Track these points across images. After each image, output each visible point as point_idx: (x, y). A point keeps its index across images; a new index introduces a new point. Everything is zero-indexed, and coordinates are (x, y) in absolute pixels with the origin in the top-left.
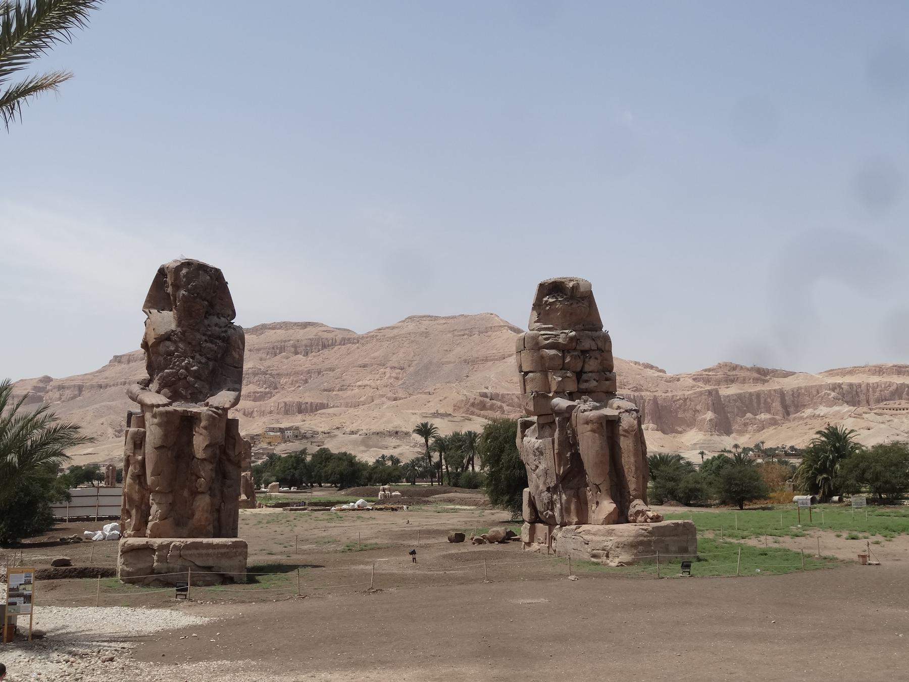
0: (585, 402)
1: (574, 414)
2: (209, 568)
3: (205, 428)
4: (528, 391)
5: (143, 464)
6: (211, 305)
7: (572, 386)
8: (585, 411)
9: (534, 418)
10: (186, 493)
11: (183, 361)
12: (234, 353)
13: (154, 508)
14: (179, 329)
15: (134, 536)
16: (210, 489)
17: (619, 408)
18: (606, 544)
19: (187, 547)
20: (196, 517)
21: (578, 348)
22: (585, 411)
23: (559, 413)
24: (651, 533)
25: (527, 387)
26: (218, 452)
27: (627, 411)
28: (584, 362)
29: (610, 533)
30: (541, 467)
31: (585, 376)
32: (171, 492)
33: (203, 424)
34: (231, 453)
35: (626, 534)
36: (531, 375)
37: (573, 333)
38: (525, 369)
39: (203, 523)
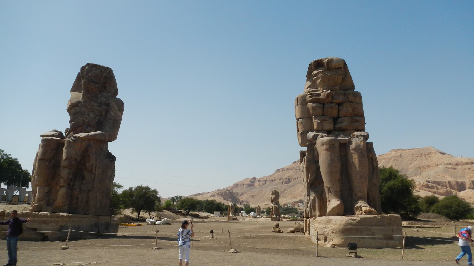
2: (35, 230)
6: (105, 87)
7: (329, 126)
9: (305, 149)
12: (111, 112)
14: (83, 100)
16: (69, 185)
18: (325, 230)
20: (58, 200)
21: (333, 101)
22: (322, 137)
26: (74, 162)
28: (339, 110)
29: (329, 222)
31: (339, 120)
33: (66, 145)
35: (338, 223)
37: (329, 91)
39: (61, 204)
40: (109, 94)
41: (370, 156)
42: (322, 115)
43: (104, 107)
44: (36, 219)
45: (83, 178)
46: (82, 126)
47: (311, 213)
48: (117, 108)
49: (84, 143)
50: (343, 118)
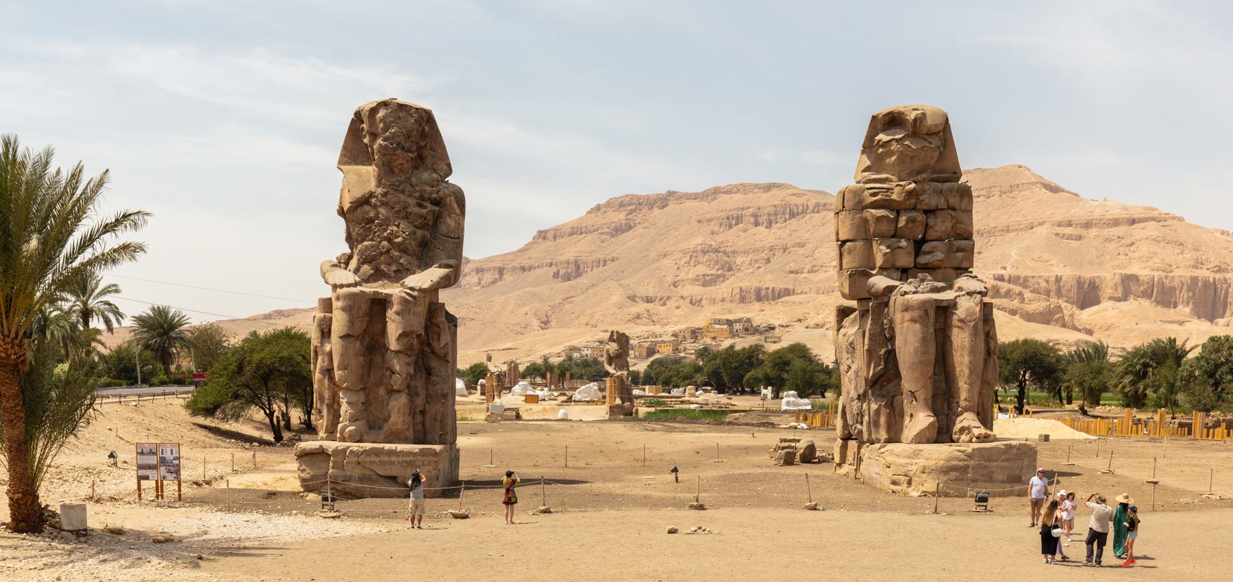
0: (923, 280)
1: (893, 298)
3: (398, 313)
4: (844, 266)
5: (330, 354)
8: (906, 293)
10: (382, 391)
11: (385, 230)
13: (345, 408)
14: (380, 190)
15: (327, 439)
16: (408, 387)
17: (960, 289)
19: (368, 453)
20: (392, 419)
22: (906, 293)
23: (877, 296)
24: (970, 456)
25: (844, 262)
26: (415, 342)
27: (968, 294)
30: (854, 367)
31: (926, 247)
32: (364, 389)
33: (396, 308)
34: (435, 344)
36: (848, 244)
38: (842, 237)
39: (400, 427)
40: (435, 176)
41: (987, 328)
42: (893, 236)
43: (430, 207)
44: (394, 459)
45: (429, 372)
46: (388, 252)
47: (870, 434)
48: (458, 211)
49: (427, 300)
50: (934, 243)
